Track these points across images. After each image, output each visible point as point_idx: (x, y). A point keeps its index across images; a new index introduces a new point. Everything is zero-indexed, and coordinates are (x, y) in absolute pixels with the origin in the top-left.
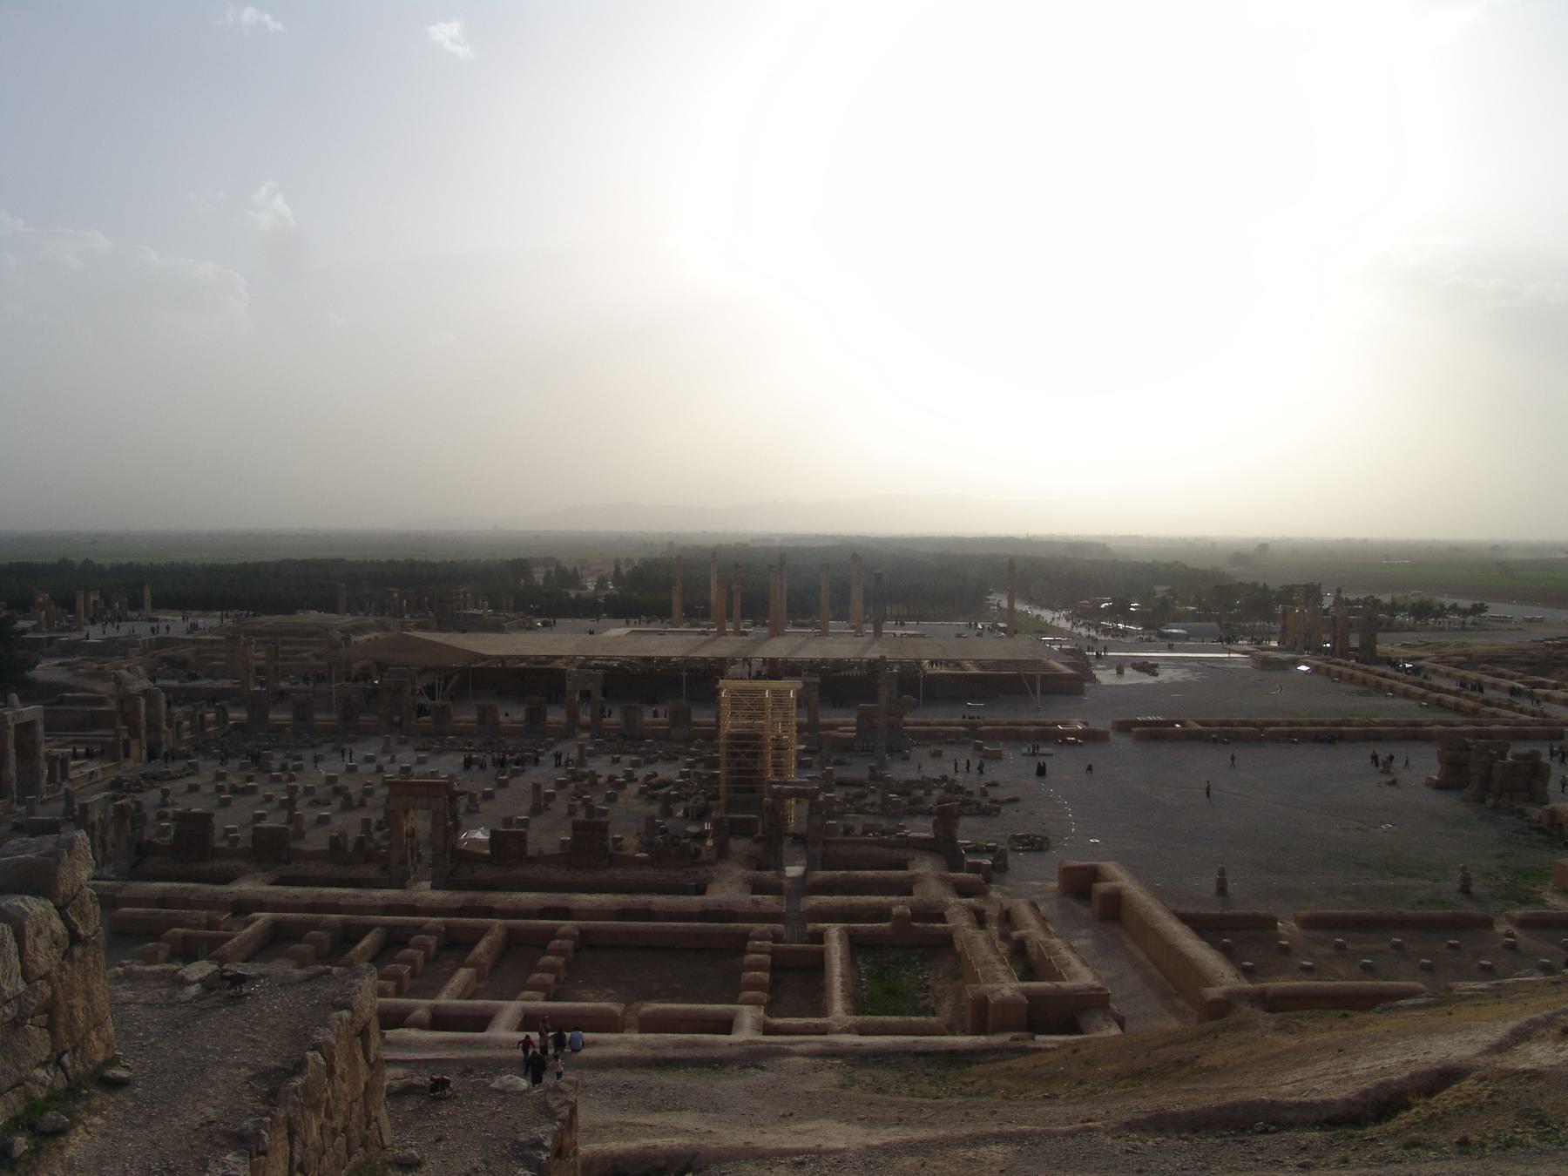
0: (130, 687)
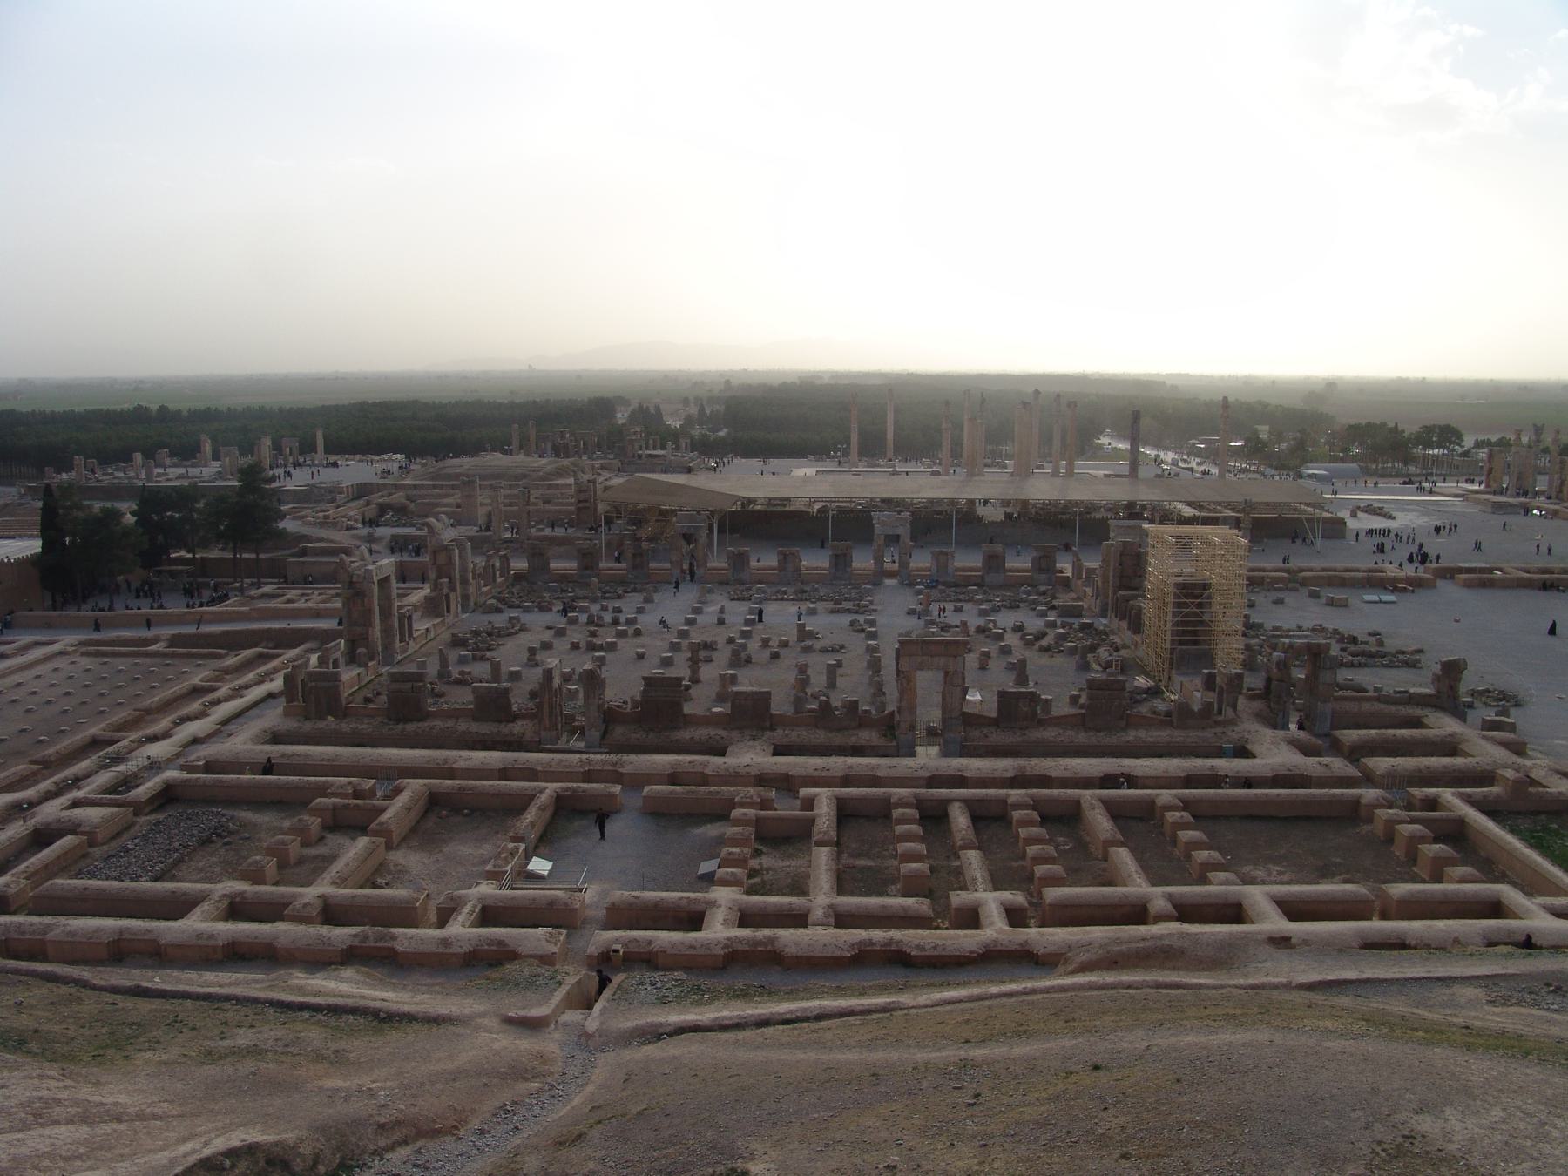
0: (443, 537)
